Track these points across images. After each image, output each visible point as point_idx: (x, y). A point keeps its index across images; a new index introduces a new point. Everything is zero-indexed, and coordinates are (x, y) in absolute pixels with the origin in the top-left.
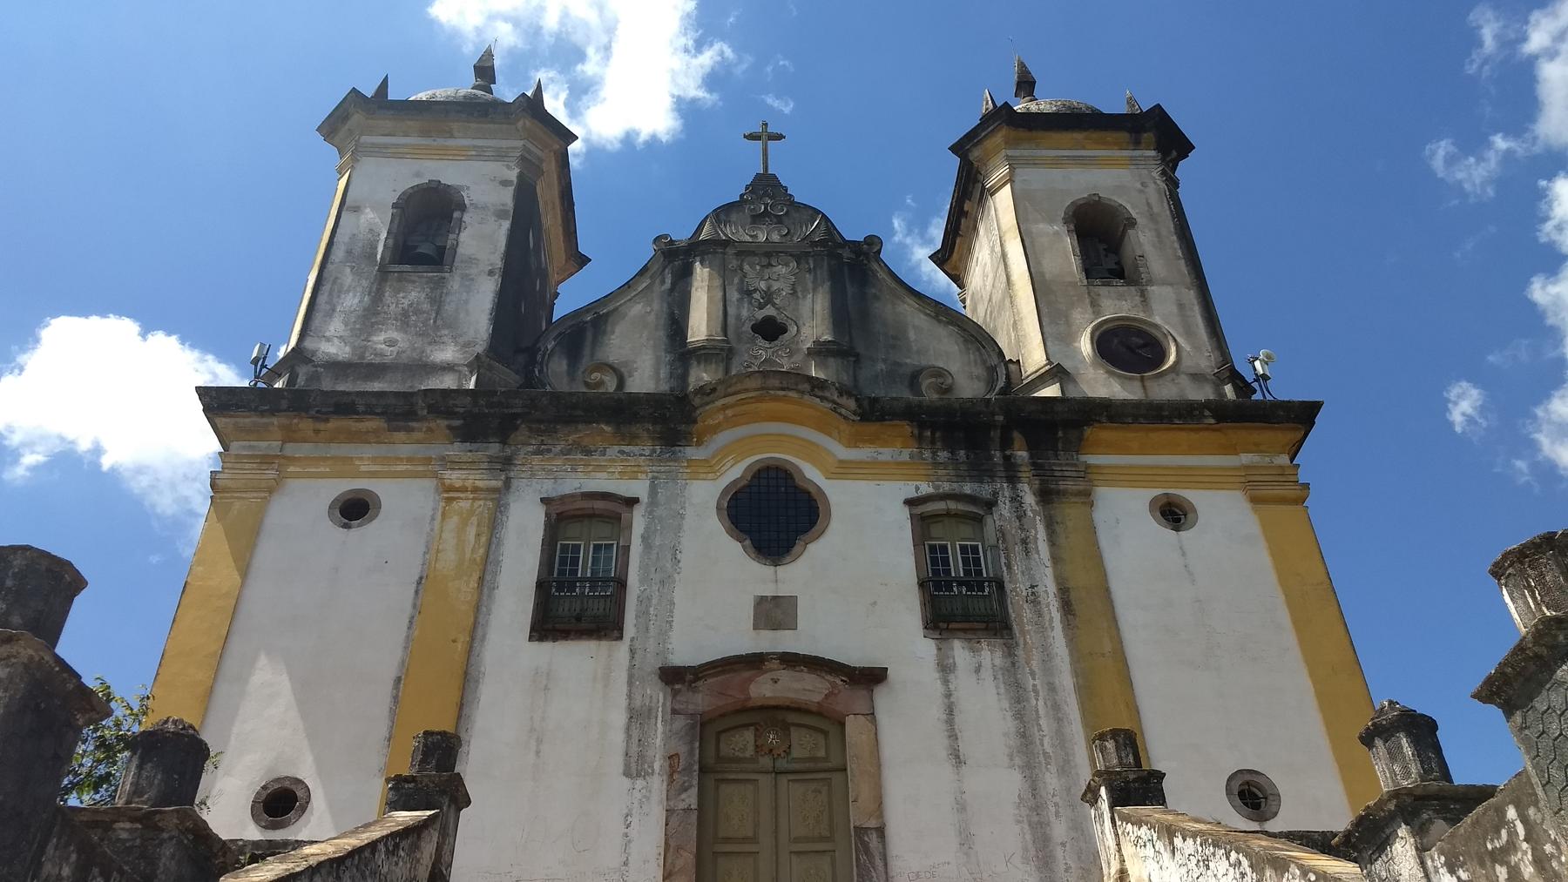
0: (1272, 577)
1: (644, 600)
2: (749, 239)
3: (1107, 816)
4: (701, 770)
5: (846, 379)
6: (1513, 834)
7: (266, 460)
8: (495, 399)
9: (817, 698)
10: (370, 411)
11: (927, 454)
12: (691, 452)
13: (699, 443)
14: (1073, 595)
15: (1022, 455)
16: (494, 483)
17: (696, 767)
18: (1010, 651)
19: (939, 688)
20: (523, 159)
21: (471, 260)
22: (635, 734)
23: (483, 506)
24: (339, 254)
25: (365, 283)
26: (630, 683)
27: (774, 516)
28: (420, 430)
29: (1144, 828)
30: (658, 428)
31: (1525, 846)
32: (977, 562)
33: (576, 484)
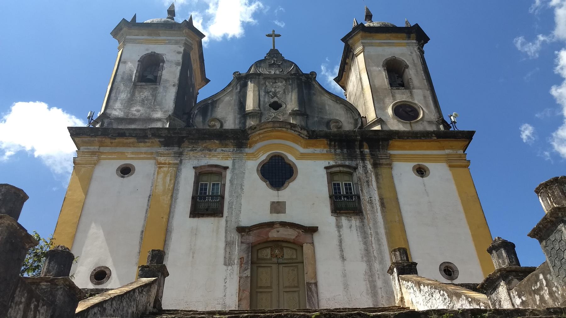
0: (456, 194)
1: (231, 204)
2: (268, 73)
3: (396, 278)
4: (252, 263)
5: (303, 123)
6: (542, 284)
7: (93, 153)
8: (176, 131)
9: (293, 237)
10: (131, 136)
11: (333, 151)
12: (247, 150)
13: (250, 147)
14: (385, 200)
15: (367, 151)
16: (176, 161)
17: (250, 262)
18: (362, 220)
20: (185, 44)
21: (167, 81)
22: (228, 250)
23: (172, 170)
24: (119, 78)
25: (128, 89)
26: (226, 233)
27: (278, 173)
28: (149, 142)
29: (410, 282)
30: (235, 141)
31: (546, 288)
32: (350, 189)
33: (206, 162)
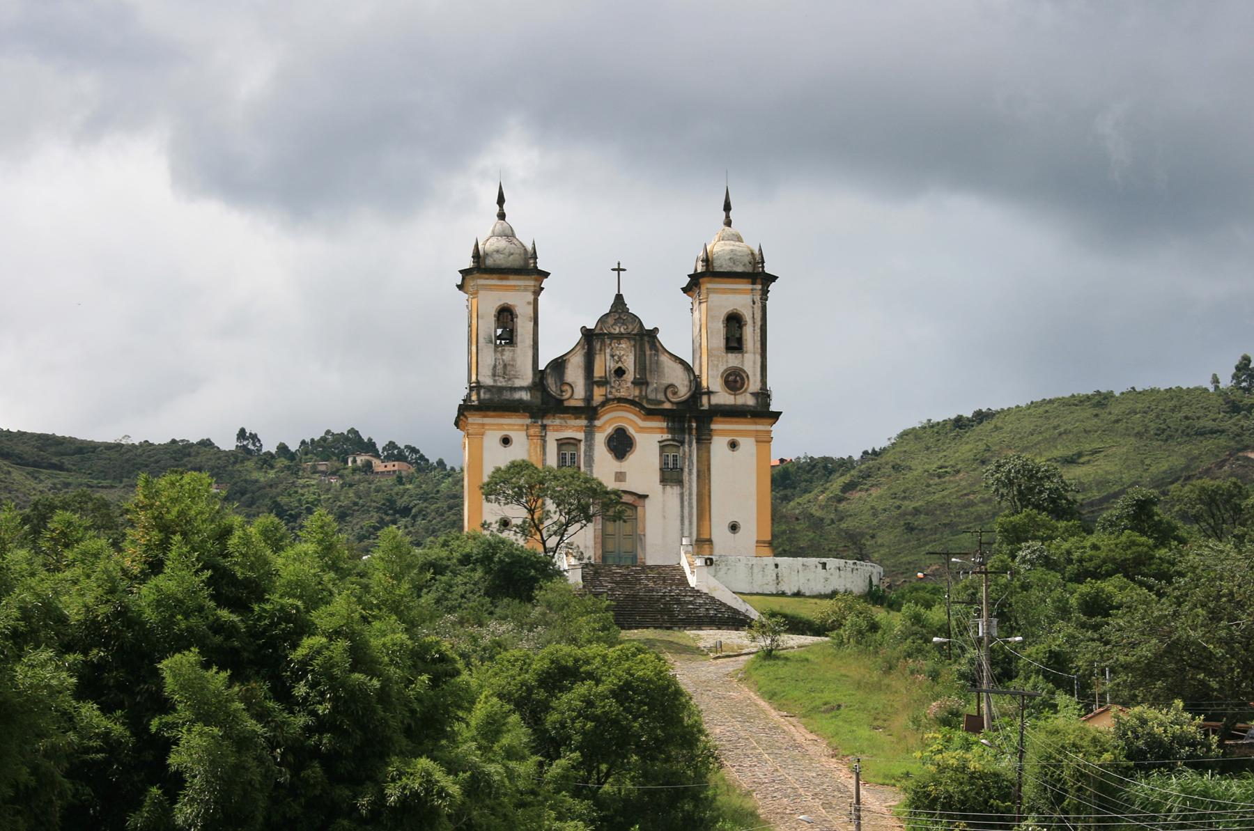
12: (597, 423)
15: (694, 425)
24: (481, 340)
27: (621, 444)
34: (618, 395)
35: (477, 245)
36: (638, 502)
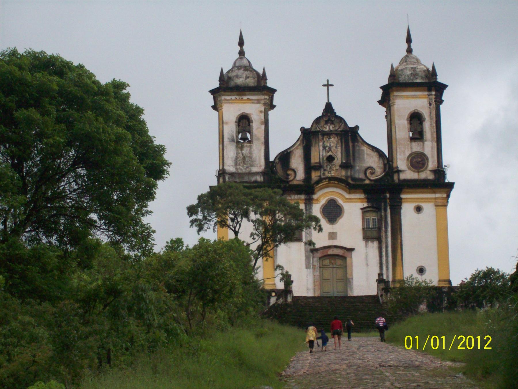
4: (320, 267)
15: (388, 195)
18: (380, 243)
19: (365, 251)
24: (226, 140)
27: (333, 212)
34: (329, 175)
35: (222, 71)
36: (347, 254)
